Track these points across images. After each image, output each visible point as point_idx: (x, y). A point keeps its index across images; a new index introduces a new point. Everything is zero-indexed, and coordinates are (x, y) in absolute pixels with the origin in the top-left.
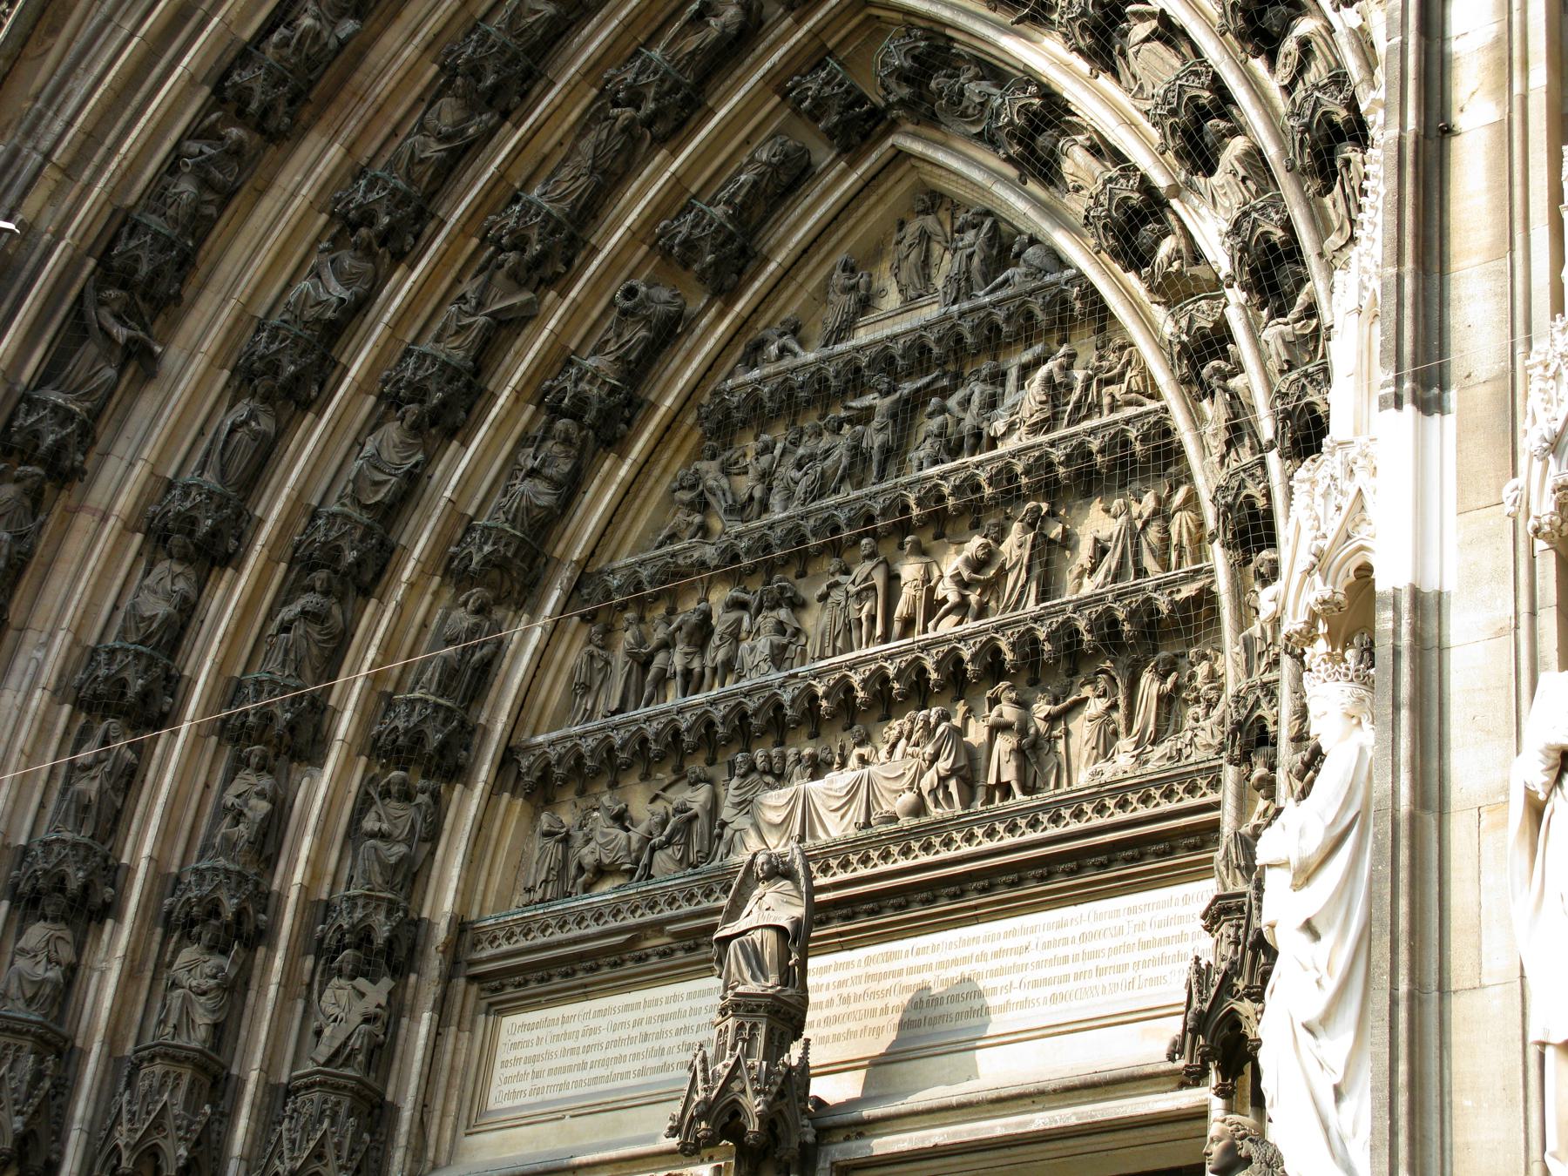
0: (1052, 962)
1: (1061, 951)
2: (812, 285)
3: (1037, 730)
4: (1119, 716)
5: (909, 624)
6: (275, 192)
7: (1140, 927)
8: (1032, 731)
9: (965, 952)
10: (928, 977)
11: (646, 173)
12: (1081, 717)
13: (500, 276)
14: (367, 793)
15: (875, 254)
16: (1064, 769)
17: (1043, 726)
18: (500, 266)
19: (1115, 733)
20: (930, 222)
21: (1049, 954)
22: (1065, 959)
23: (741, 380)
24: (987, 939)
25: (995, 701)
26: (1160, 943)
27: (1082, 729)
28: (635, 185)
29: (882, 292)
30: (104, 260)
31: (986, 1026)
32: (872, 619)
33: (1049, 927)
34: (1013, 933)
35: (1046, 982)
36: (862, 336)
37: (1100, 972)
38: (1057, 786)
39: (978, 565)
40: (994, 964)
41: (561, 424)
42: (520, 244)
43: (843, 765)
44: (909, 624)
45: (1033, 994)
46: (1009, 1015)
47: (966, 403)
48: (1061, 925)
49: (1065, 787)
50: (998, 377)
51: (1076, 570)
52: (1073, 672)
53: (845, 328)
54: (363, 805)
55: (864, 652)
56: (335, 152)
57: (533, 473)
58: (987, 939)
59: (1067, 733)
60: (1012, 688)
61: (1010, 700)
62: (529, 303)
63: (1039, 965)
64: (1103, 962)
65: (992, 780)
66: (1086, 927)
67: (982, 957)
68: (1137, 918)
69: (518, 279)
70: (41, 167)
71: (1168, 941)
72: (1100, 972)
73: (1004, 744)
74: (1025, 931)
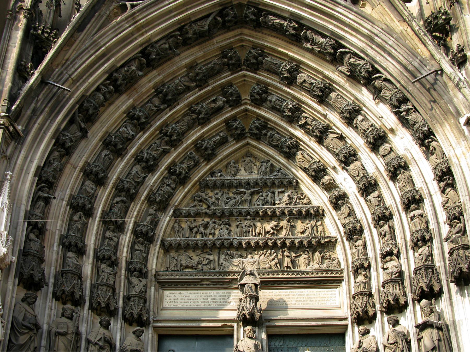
1: (302, 296)
2: (224, 164)
5: (259, 234)
6: (114, 105)
10: (272, 297)
11: (196, 130)
12: (301, 258)
13: (163, 141)
14: (135, 242)
15: (236, 162)
18: (163, 139)
20: (251, 159)
23: (210, 179)
24: (285, 292)
28: (193, 132)
29: (240, 170)
30: (81, 106)
32: (252, 231)
33: (299, 292)
34: (291, 292)
35: (300, 301)
36: (238, 177)
39: (276, 226)
40: (288, 297)
41: (174, 177)
42: (171, 136)
43: (246, 257)
44: (259, 234)
45: (297, 303)
47: (267, 196)
48: (302, 292)
50: (273, 193)
53: (235, 175)
54: (134, 243)
55: (251, 237)
56: (131, 101)
57: (168, 185)
58: (285, 292)
62: (169, 149)
64: (312, 299)
66: (307, 293)
67: (284, 295)
69: (167, 143)
70: (68, 79)
72: (311, 301)
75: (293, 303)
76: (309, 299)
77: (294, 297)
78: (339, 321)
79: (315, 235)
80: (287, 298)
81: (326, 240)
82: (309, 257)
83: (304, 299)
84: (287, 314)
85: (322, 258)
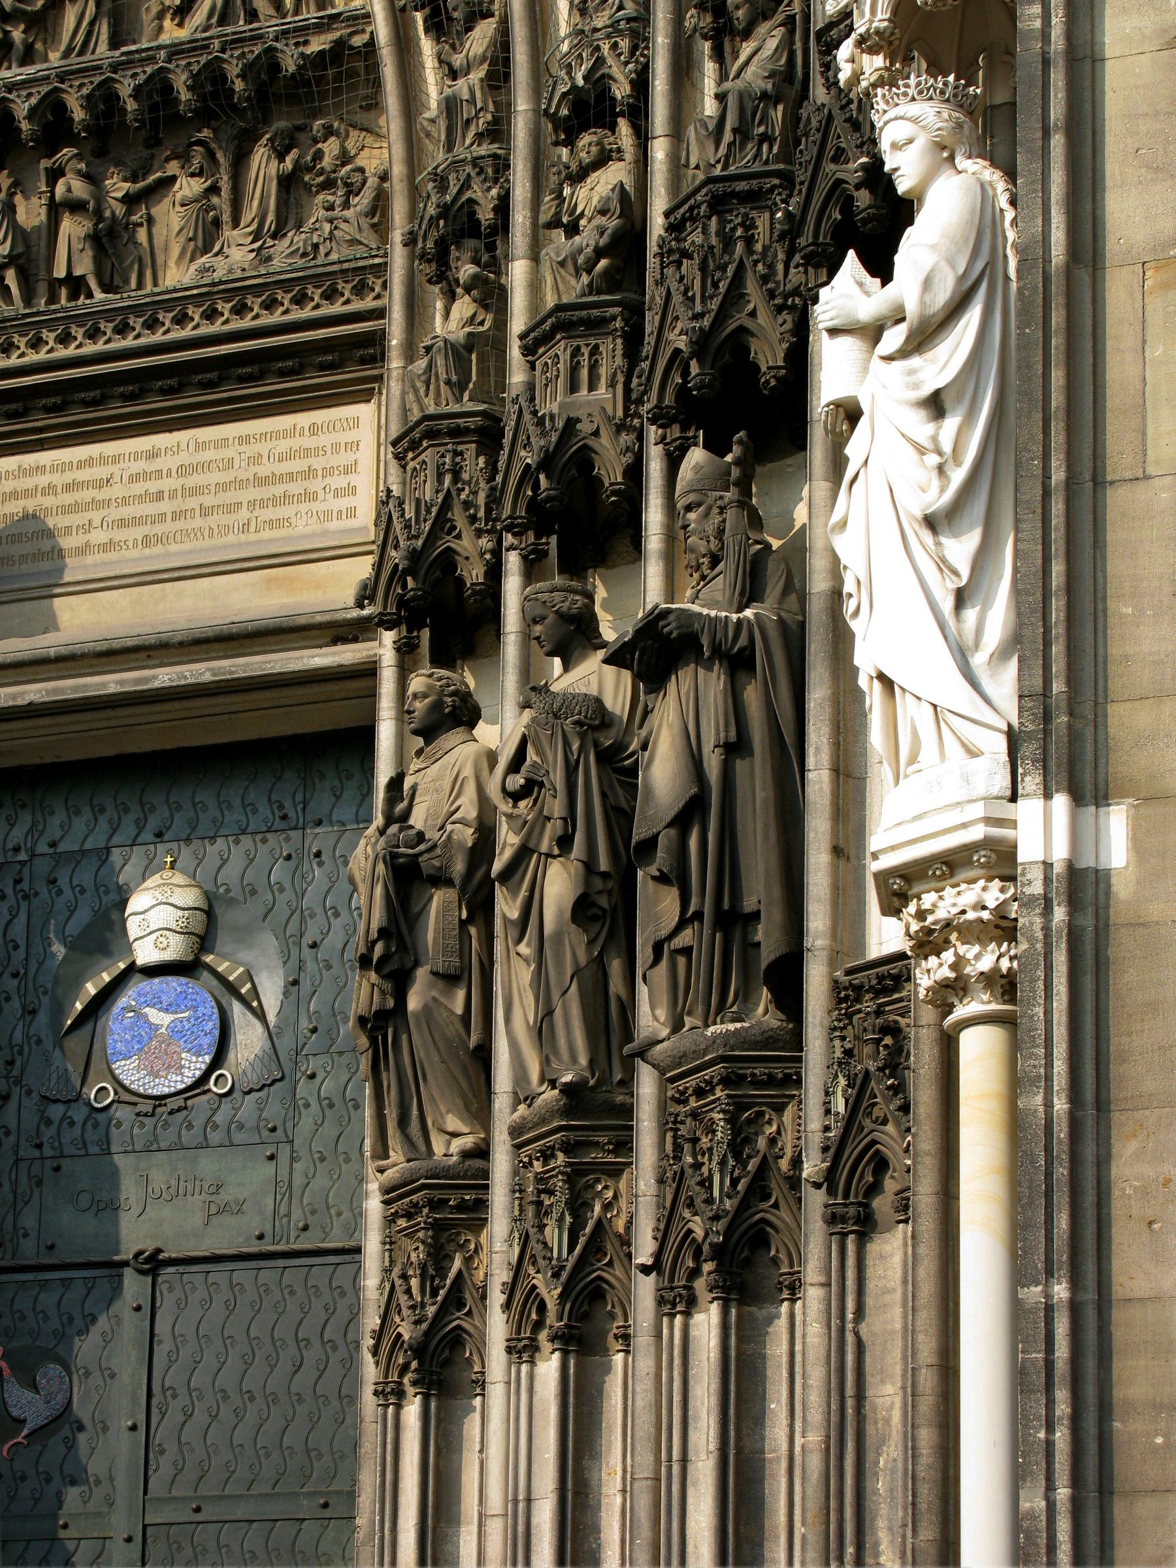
0: (141, 499)
1: (153, 486)
3: (113, 213)
4: (222, 202)
7: (256, 459)
8: (107, 214)
9: (29, 483)
12: (167, 201)
16: (151, 264)
17: (120, 210)
19: (217, 223)
21: (139, 488)
22: (159, 496)
24: (54, 469)
25: (55, 175)
26: (281, 479)
27: (171, 219)
31: (61, 570)
33: (137, 456)
35: (137, 521)
37: (205, 512)
38: (140, 286)
40: (67, 499)
45: (119, 535)
46: (89, 559)
48: (153, 455)
49: (149, 288)
51: (155, 10)
52: (154, 142)
58: (54, 469)
59: (150, 221)
60: (79, 157)
61: (79, 173)
63: (125, 501)
64: (208, 500)
65: (60, 272)
66: (184, 458)
67: (50, 489)
68: (250, 450)
71: (291, 477)
72: (205, 512)
73: (71, 228)
74: (104, 460)
75: (98, 536)
76: (193, 503)
77: (101, 495)
78: (337, 640)
79: (252, 15)
80: (66, 510)
81: (317, 44)
82: (214, 190)
83: (165, 506)
84: (51, 624)
85: (288, 183)
